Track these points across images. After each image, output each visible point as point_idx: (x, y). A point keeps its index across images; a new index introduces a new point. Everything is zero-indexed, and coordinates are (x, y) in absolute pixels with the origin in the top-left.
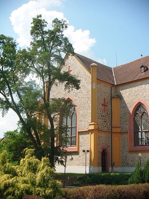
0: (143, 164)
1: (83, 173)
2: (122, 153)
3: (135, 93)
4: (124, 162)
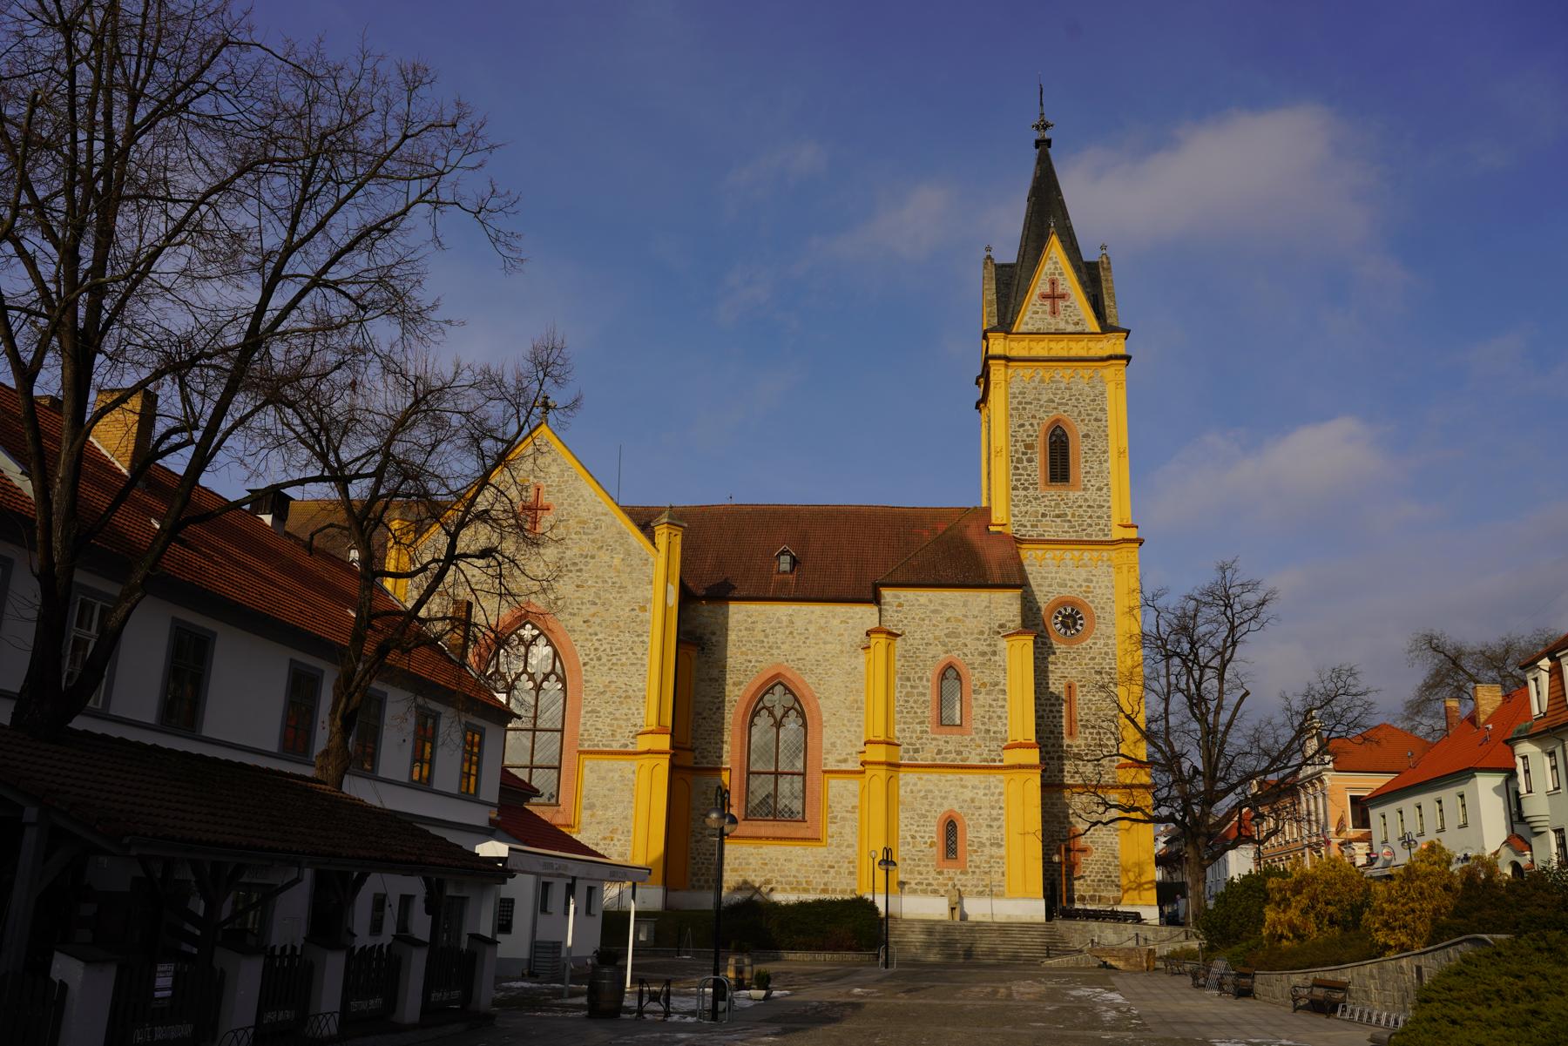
0: (777, 882)
1: (937, 917)
2: (697, 842)
3: (765, 640)
4: (703, 874)
